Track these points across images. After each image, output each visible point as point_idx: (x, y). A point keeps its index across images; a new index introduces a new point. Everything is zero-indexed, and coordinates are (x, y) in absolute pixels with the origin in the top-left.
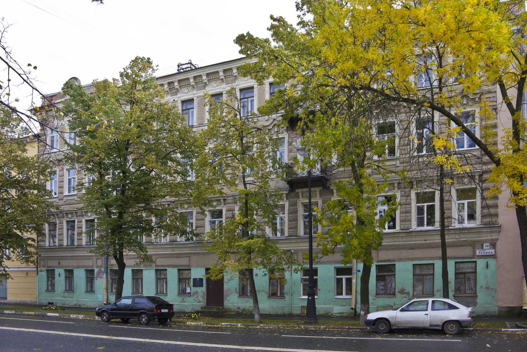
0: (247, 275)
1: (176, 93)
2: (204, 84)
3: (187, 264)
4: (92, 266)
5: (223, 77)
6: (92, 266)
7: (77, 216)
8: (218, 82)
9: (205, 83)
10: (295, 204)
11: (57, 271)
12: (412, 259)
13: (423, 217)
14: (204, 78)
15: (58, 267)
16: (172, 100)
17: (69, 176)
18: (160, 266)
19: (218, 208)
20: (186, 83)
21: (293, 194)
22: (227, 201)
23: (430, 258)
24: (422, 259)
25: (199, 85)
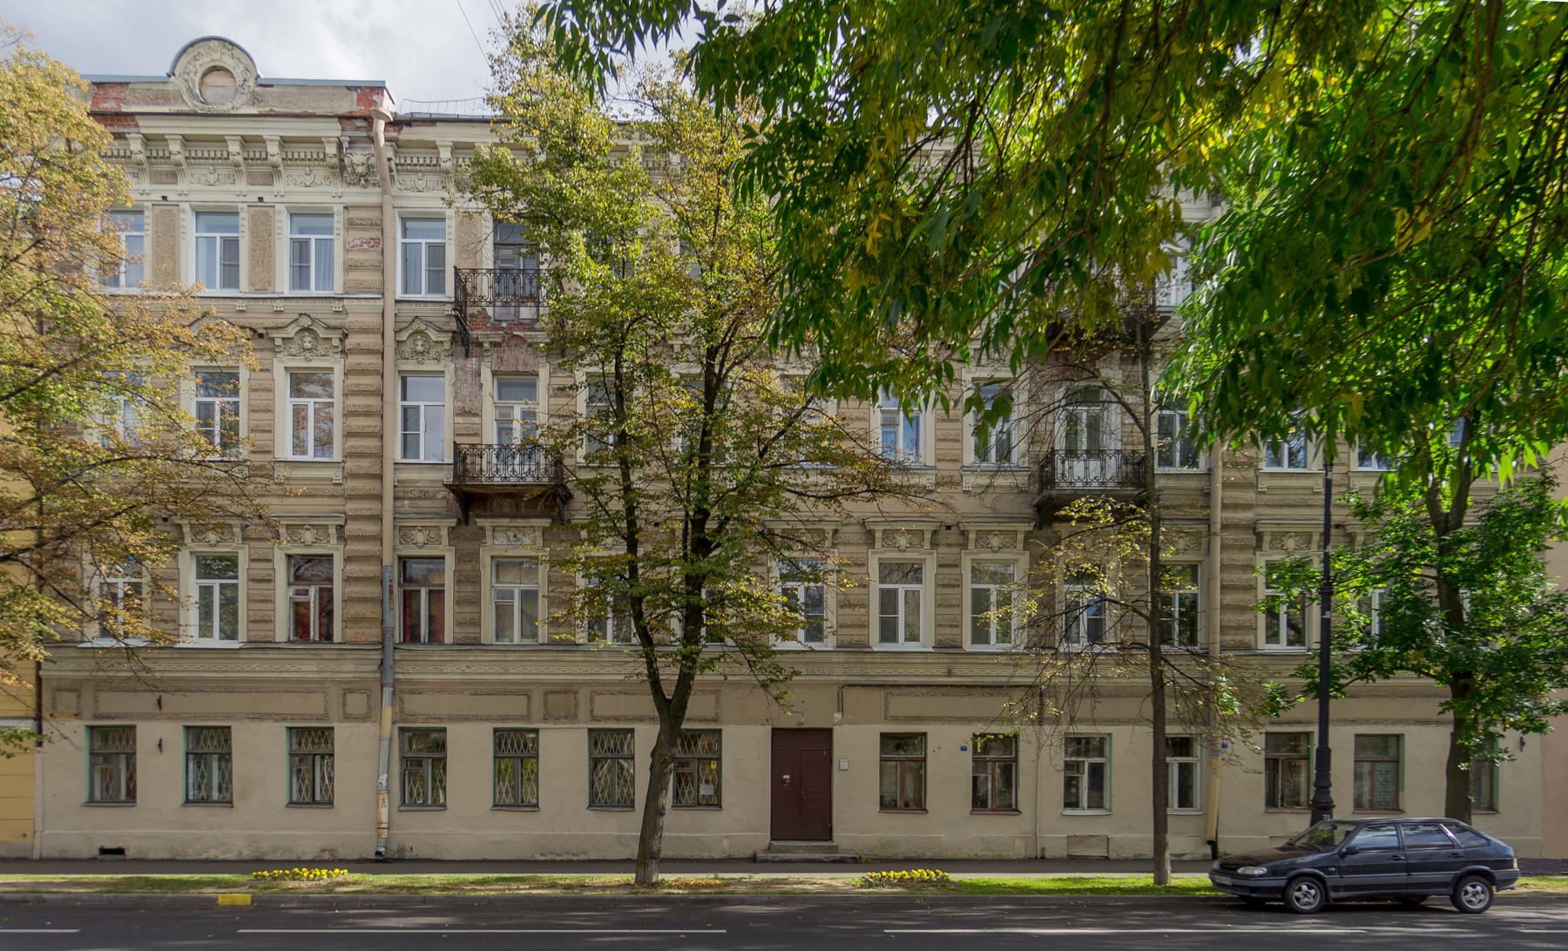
0: (901, 747)
1: (173, 177)
2: (270, 169)
3: (710, 714)
4: (325, 716)
5: (239, 159)
6: (325, 716)
7: (244, 539)
8: (222, 171)
9: (275, 166)
10: (474, 557)
11: (147, 734)
12: (1353, 722)
13: (896, 619)
14: (273, 148)
15: (150, 717)
16: (157, 197)
17: (404, 398)
18: (608, 719)
19: (223, 549)
20: (421, 157)
21: (465, 530)
22: (841, 537)
23: (1395, 722)
24: (1377, 722)
25: (255, 169)
